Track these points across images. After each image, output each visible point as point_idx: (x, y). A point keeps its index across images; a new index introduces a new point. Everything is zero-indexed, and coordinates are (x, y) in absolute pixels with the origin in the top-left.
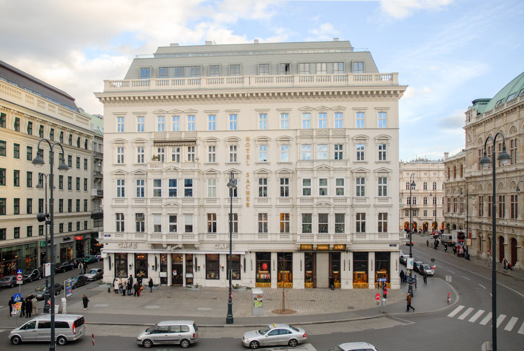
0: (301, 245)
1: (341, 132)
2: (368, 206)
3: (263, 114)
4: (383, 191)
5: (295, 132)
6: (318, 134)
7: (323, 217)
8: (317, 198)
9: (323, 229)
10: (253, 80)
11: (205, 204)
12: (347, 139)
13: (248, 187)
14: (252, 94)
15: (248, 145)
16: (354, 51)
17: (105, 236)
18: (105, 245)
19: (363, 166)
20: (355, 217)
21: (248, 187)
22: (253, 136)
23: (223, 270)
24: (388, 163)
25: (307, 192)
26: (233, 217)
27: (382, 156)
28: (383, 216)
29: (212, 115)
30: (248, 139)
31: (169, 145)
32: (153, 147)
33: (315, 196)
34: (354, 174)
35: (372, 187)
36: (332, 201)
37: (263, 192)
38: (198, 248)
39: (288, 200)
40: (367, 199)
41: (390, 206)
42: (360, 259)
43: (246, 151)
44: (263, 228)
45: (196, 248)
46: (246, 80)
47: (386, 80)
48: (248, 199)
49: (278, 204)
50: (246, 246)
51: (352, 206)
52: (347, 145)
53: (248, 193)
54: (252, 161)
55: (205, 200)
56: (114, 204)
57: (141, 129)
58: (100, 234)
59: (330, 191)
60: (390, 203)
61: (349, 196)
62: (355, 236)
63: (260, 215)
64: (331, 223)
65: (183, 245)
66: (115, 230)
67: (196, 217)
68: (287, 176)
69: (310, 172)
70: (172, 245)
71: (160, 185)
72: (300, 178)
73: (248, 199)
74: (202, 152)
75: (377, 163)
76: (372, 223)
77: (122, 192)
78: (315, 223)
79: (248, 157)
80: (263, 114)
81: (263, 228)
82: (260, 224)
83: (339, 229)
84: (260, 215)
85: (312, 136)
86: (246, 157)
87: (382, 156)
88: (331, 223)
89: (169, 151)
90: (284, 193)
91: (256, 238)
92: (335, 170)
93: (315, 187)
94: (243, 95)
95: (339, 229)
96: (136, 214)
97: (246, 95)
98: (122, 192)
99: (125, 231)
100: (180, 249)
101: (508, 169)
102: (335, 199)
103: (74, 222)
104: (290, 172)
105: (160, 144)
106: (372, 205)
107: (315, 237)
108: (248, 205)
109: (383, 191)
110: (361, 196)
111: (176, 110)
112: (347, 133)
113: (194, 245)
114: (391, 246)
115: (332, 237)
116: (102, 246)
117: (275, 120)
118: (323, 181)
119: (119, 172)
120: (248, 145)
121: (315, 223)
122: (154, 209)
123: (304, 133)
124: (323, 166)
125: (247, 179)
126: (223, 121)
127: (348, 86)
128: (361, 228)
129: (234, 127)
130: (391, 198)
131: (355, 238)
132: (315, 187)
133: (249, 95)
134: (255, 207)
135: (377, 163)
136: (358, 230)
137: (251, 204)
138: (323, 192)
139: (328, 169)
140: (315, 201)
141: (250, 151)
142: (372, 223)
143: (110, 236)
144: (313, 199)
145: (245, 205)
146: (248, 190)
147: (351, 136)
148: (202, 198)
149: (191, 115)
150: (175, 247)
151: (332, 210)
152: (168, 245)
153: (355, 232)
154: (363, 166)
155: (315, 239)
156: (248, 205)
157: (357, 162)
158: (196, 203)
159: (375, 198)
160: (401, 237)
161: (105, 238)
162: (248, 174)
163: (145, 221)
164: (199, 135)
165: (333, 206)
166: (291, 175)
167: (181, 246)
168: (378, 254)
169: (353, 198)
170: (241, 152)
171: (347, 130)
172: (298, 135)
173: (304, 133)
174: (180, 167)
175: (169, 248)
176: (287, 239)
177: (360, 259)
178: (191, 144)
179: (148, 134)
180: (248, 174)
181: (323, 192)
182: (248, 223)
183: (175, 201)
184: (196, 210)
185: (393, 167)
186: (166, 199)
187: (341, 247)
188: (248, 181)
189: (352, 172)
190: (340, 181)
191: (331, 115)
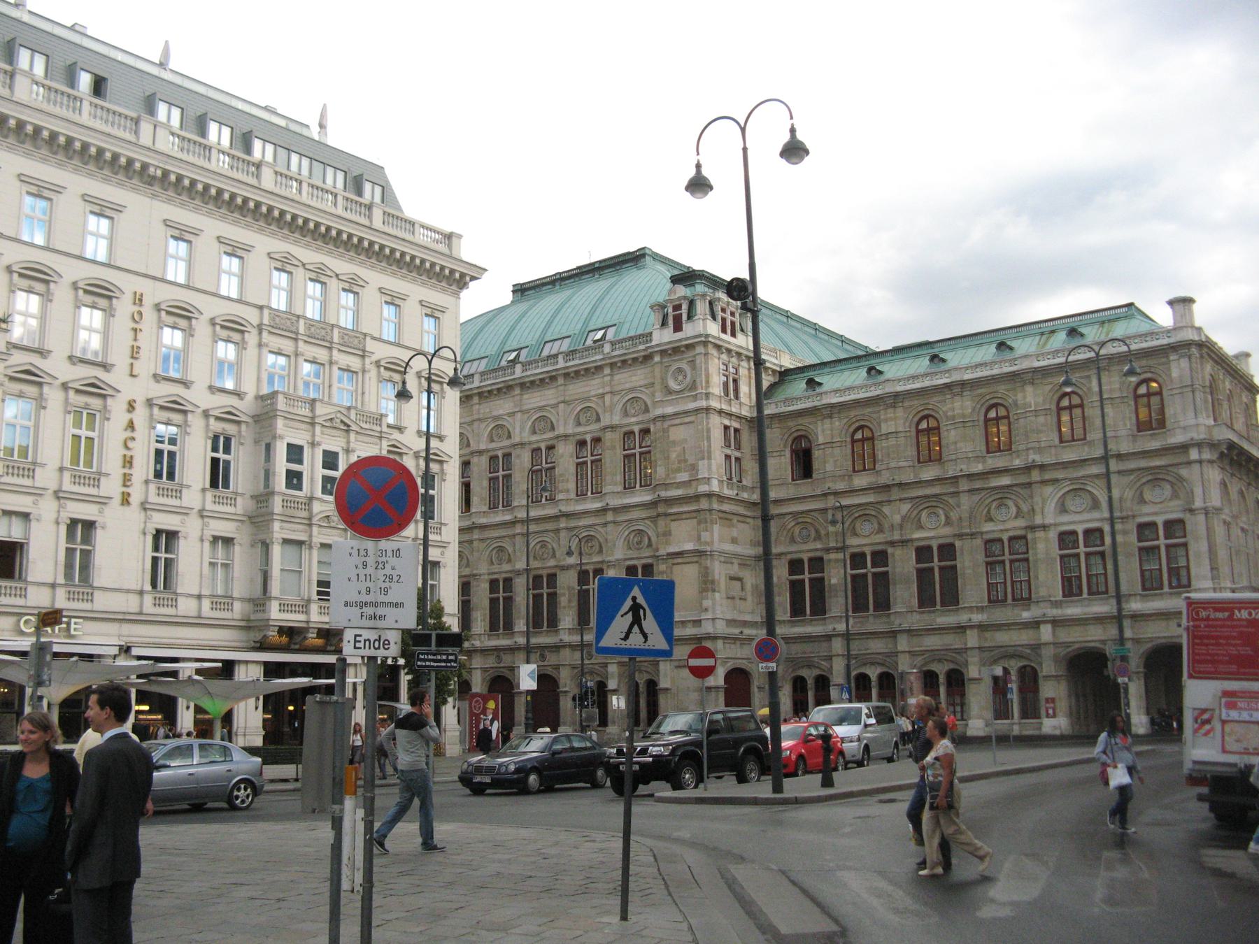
14: (166, 173)
15: (137, 318)
21: (130, 444)
25: (294, 479)
30: (138, 300)
43: (132, 333)
48: (126, 480)
50: (113, 628)
53: (128, 462)
54: (145, 367)
68: (231, 429)
69: (304, 426)
72: (281, 437)
73: (126, 480)
79: (135, 353)
86: (128, 352)
94: (145, 166)
97: (152, 170)
104: (244, 418)
108: (125, 500)
112: (370, 345)
120: (137, 318)
123: (277, 320)
125: (128, 416)
133: (159, 173)
134: (144, 506)
141: (139, 335)
146: (129, 453)
147: (374, 358)
156: (125, 500)
176: (227, 615)
182: (121, 556)
188: (131, 426)
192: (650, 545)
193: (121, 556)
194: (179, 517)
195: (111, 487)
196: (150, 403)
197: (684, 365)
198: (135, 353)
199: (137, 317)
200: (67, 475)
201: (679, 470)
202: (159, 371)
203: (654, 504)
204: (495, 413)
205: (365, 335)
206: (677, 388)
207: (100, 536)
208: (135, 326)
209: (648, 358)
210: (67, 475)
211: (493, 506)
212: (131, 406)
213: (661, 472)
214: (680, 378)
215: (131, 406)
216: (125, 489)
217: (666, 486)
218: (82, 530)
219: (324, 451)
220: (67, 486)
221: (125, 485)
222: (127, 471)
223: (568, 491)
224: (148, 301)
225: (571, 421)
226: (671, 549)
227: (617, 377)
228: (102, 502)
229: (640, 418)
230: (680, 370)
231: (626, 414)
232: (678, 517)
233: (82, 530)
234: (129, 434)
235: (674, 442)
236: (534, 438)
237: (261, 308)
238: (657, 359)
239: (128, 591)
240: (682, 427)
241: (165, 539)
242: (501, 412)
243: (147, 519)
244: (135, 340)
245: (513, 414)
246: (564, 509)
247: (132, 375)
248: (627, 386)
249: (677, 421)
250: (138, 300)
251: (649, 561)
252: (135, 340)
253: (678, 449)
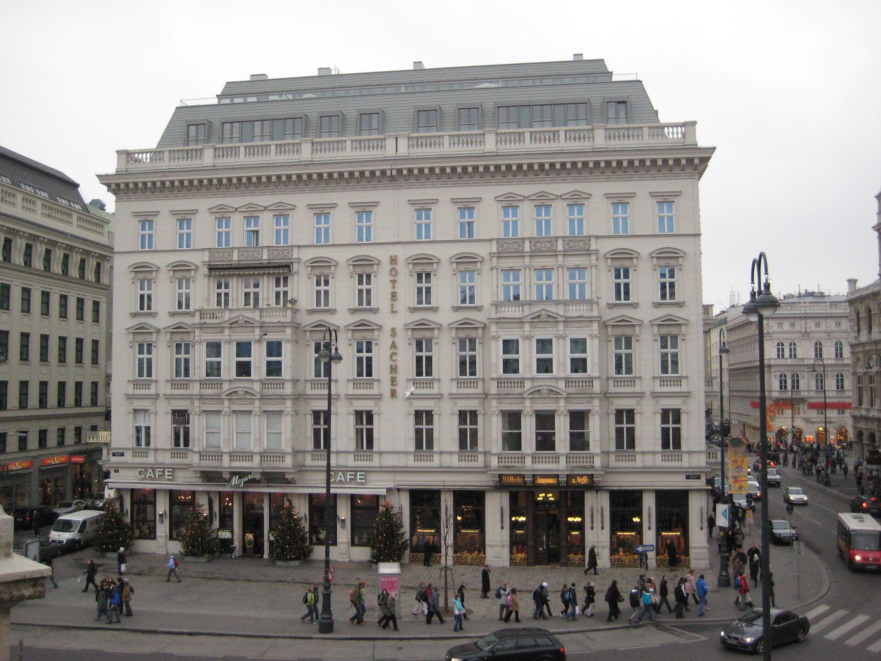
0: (500, 476)
1: (582, 244)
2: (640, 396)
3: (423, 208)
4: (669, 364)
5: (487, 244)
6: (534, 249)
7: (545, 420)
8: (532, 379)
9: (545, 442)
10: (403, 143)
11: (309, 391)
12: (594, 257)
13: (394, 358)
14: (400, 171)
15: (394, 272)
16: (614, 79)
17: (114, 455)
18: (112, 474)
19: (629, 312)
20: (613, 418)
22: (403, 253)
23: (343, 527)
24: (680, 305)
25: (510, 366)
26: (365, 418)
27: (667, 290)
28: (671, 416)
29: (322, 212)
30: (393, 260)
31: (239, 275)
32: (206, 279)
33: (528, 376)
34: (610, 329)
35: (646, 355)
36: (562, 385)
37: (424, 366)
38: (293, 479)
39: (475, 382)
40: (637, 382)
41: (686, 395)
42: (625, 504)
43: (390, 285)
44: (424, 440)
45: (289, 482)
46: (390, 144)
47: (674, 135)
48: (393, 381)
49: (454, 390)
50: (391, 477)
51: (606, 396)
52: (594, 270)
53: (393, 369)
55: (309, 385)
56: (131, 391)
57: (185, 242)
58: (105, 451)
59: (558, 364)
60: (684, 388)
61: (596, 374)
62: (612, 457)
63: (418, 414)
64: (562, 429)
65: (263, 473)
66: (132, 444)
67: (289, 419)
69: (517, 325)
70: (241, 475)
71: (218, 355)
73: (393, 381)
74: (302, 288)
75: (657, 305)
76: (649, 431)
77: (145, 368)
78: (528, 429)
79: (394, 296)
80: (423, 208)
81: (424, 440)
82: (418, 432)
83: (579, 441)
84: (418, 414)
85: (523, 252)
86: (390, 296)
87: (667, 290)
88: (562, 429)
89: (237, 289)
90: (467, 366)
91: (410, 461)
92: (567, 321)
93: (528, 356)
94: (383, 172)
95: (579, 441)
97: (388, 173)
98: (145, 368)
99: (152, 446)
100: (259, 482)
102: (567, 381)
103: (70, 427)
104: (478, 325)
105: (220, 271)
106: (648, 393)
107: (528, 460)
108: (393, 394)
109: (669, 364)
110: (624, 375)
111: (250, 206)
113: (284, 473)
114: (688, 477)
115: (563, 460)
116: (107, 475)
118: (544, 345)
120: (394, 272)
121: (528, 429)
122: (208, 401)
124: (544, 312)
126: (343, 225)
127: (594, 152)
128: (626, 440)
129: (364, 237)
130: (686, 377)
131: (613, 462)
132: (528, 356)
133: (394, 173)
135: (657, 305)
136: (619, 445)
137: (399, 389)
138: (545, 366)
139: (552, 319)
140: (528, 385)
141: (397, 285)
142: (649, 431)
143: (122, 455)
144: (522, 381)
145: (387, 393)
147: (602, 252)
148: (302, 379)
149: (282, 214)
150: (246, 479)
151: (562, 403)
152: (233, 474)
153: (613, 448)
154: (629, 312)
155: (530, 462)
156: (393, 394)
157: (615, 305)
158: (288, 389)
159: (654, 378)
160: (711, 460)
161: (114, 459)
162: (393, 330)
163: (190, 426)
164: (295, 254)
165: (564, 395)
166: (480, 331)
167: (258, 477)
168: (662, 496)
169: (608, 378)
170: (380, 287)
171: (593, 240)
172: (494, 250)
173: (506, 246)
174: (257, 318)
175: (235, 480)
177: (625, 504)
178: (281, 271)
179: (200, 253)
180: (393, 330)
181: (545, 366)
182: (394, 431)
183: (247, 385)
184: (289, 403)
185: (692, 314)
186: (230, 381)
187: (584, 481)
188: (394, 346)
189: (604, 325)
190: (579, 344)
191: (559, 209)
193: (394, 431)
198: (394, 296)
205: (590, 237)
216: (392, 387)
218: (365, 418)
219: (538, 341)
221: (392, 385)
224: (401, 260)
228: (378, 398)
233: (365, 418)
237: (490, 240)
239: (400, 453)
241: (423, 417)
243: (411, 404)
244: (394, 288)
247: (393, 312)
250: (393, 260)
252: (394, 288)
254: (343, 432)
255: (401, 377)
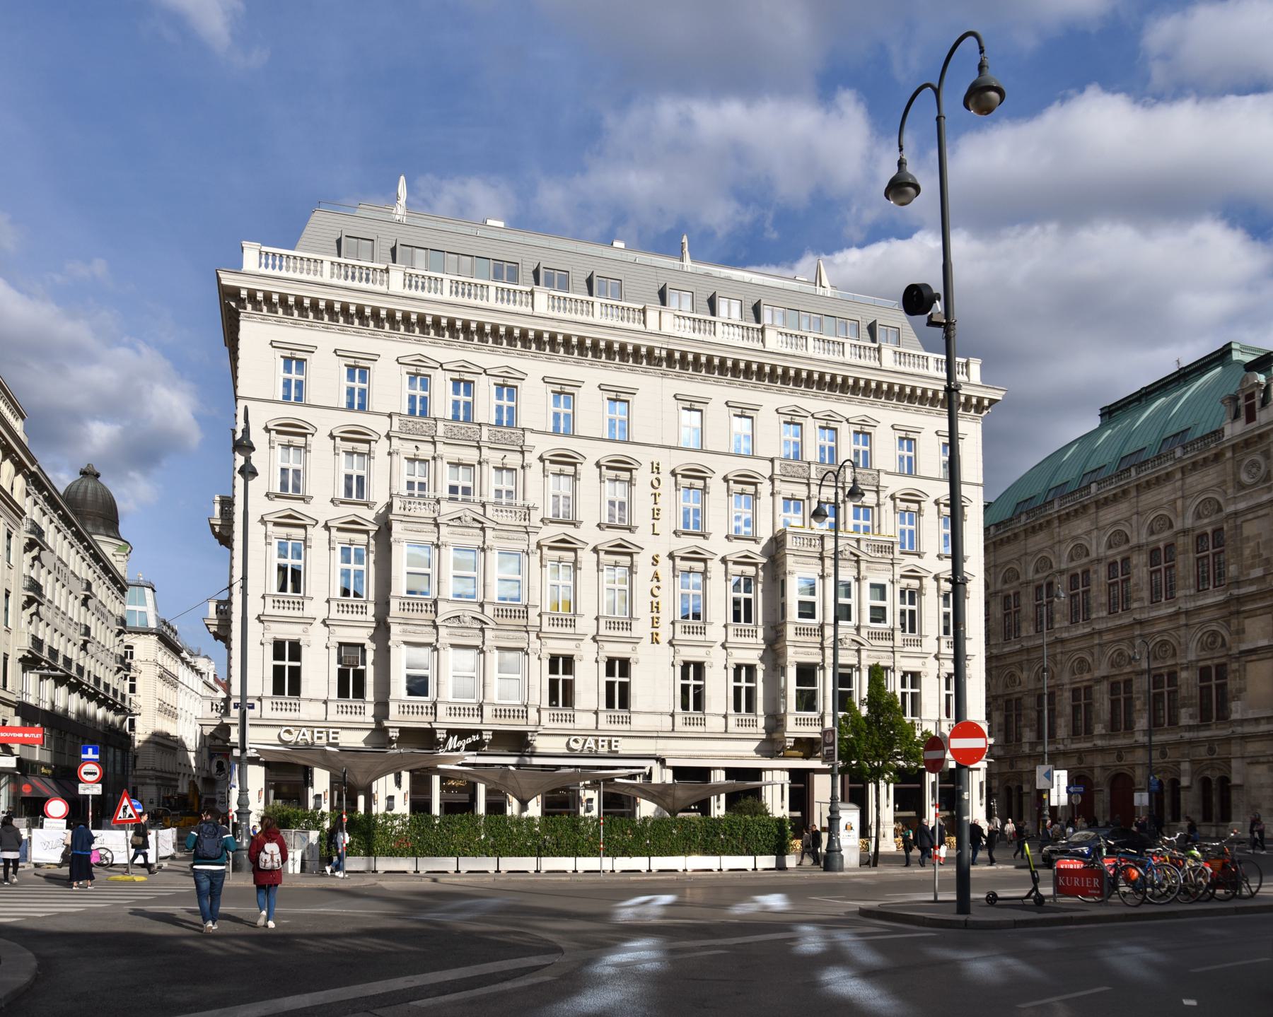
21: (656, 592)
30: (656, 468)
48: (655, 623)
53: (655, 607)
70: (463, 734)
73: (655, 623)
79: (656, 514)
96: (341, 644)
101: (1065, 635)
108: (655, 640)
117: (726, 430)
119: (290, 517)
150: (469, 741)
152: (451, 732)
156: (655, 640)
182: (654, 685)
192: (1224, 644)
194: (631, 646)
195: (642, 628)
196: (671, 556)
197: (1258, 458)
198: (656, 514)
199: (656, 483)
200: (269, 600)
201: (1252, 566)
202: (680, 527)
203: (1226, 603)
204: (1074, 534)
206: (1251, 481)
207: (634, 669)
208: (654, 491)
209: (1218, 457)
210: (269, 600)
211: (1074, 622)
212: (655, 561)
213: (1232, 570)
214: (1254, 470)
215: (655, 561)
216: (655, 630)
217: (1238, 583)
220: (334, 615)
222: (655, 615)
223: (1142, 599)
225: (1144, 531)
226: (1244, 647)
227: (1189, 480)
228: (635, 642)
229: (1213, 518)
230: (1254, 464)
231: (1198, 516)
232: (1252, 614)
234: (655, 583)
235: (1248, 538)
236: (1110, 552)
238: (1229, 455)
239: (662, 714)
240: (1256, 521)
242: (1080, 531)
245: (1088, 533)
246: (1137, 617)
248: (1200, 487)
249: (1250, 516)
250: (656, 468)
251: (1224, 660)
253: (1252, 544)
254: (589, 683)
255: (665, 617)
